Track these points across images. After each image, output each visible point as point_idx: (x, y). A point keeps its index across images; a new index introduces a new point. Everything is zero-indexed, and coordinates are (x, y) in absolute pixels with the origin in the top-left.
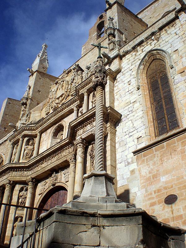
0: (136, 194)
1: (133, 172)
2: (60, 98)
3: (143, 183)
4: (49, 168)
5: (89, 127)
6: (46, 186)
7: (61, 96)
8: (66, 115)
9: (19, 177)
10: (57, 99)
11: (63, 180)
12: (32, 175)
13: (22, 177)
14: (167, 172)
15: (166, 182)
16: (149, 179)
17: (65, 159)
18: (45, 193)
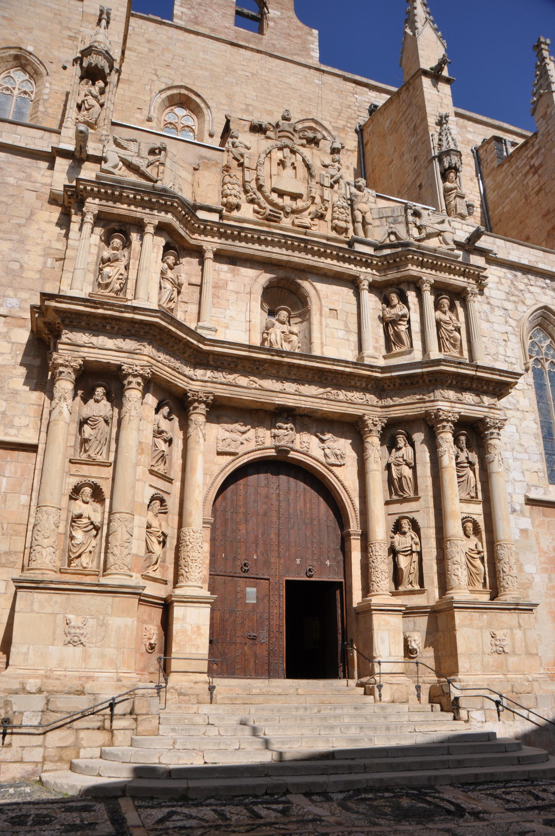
0: (533, 578)
1: (524, 532)
2: (287, 199)
3: (544, 563)
4: (290, 401)
5: (469, 397)
6: (245, 436)
7: (295, 197)
8: (321, 272)
9: (170, 370)
10: (274, 190)
13: (177, 375)
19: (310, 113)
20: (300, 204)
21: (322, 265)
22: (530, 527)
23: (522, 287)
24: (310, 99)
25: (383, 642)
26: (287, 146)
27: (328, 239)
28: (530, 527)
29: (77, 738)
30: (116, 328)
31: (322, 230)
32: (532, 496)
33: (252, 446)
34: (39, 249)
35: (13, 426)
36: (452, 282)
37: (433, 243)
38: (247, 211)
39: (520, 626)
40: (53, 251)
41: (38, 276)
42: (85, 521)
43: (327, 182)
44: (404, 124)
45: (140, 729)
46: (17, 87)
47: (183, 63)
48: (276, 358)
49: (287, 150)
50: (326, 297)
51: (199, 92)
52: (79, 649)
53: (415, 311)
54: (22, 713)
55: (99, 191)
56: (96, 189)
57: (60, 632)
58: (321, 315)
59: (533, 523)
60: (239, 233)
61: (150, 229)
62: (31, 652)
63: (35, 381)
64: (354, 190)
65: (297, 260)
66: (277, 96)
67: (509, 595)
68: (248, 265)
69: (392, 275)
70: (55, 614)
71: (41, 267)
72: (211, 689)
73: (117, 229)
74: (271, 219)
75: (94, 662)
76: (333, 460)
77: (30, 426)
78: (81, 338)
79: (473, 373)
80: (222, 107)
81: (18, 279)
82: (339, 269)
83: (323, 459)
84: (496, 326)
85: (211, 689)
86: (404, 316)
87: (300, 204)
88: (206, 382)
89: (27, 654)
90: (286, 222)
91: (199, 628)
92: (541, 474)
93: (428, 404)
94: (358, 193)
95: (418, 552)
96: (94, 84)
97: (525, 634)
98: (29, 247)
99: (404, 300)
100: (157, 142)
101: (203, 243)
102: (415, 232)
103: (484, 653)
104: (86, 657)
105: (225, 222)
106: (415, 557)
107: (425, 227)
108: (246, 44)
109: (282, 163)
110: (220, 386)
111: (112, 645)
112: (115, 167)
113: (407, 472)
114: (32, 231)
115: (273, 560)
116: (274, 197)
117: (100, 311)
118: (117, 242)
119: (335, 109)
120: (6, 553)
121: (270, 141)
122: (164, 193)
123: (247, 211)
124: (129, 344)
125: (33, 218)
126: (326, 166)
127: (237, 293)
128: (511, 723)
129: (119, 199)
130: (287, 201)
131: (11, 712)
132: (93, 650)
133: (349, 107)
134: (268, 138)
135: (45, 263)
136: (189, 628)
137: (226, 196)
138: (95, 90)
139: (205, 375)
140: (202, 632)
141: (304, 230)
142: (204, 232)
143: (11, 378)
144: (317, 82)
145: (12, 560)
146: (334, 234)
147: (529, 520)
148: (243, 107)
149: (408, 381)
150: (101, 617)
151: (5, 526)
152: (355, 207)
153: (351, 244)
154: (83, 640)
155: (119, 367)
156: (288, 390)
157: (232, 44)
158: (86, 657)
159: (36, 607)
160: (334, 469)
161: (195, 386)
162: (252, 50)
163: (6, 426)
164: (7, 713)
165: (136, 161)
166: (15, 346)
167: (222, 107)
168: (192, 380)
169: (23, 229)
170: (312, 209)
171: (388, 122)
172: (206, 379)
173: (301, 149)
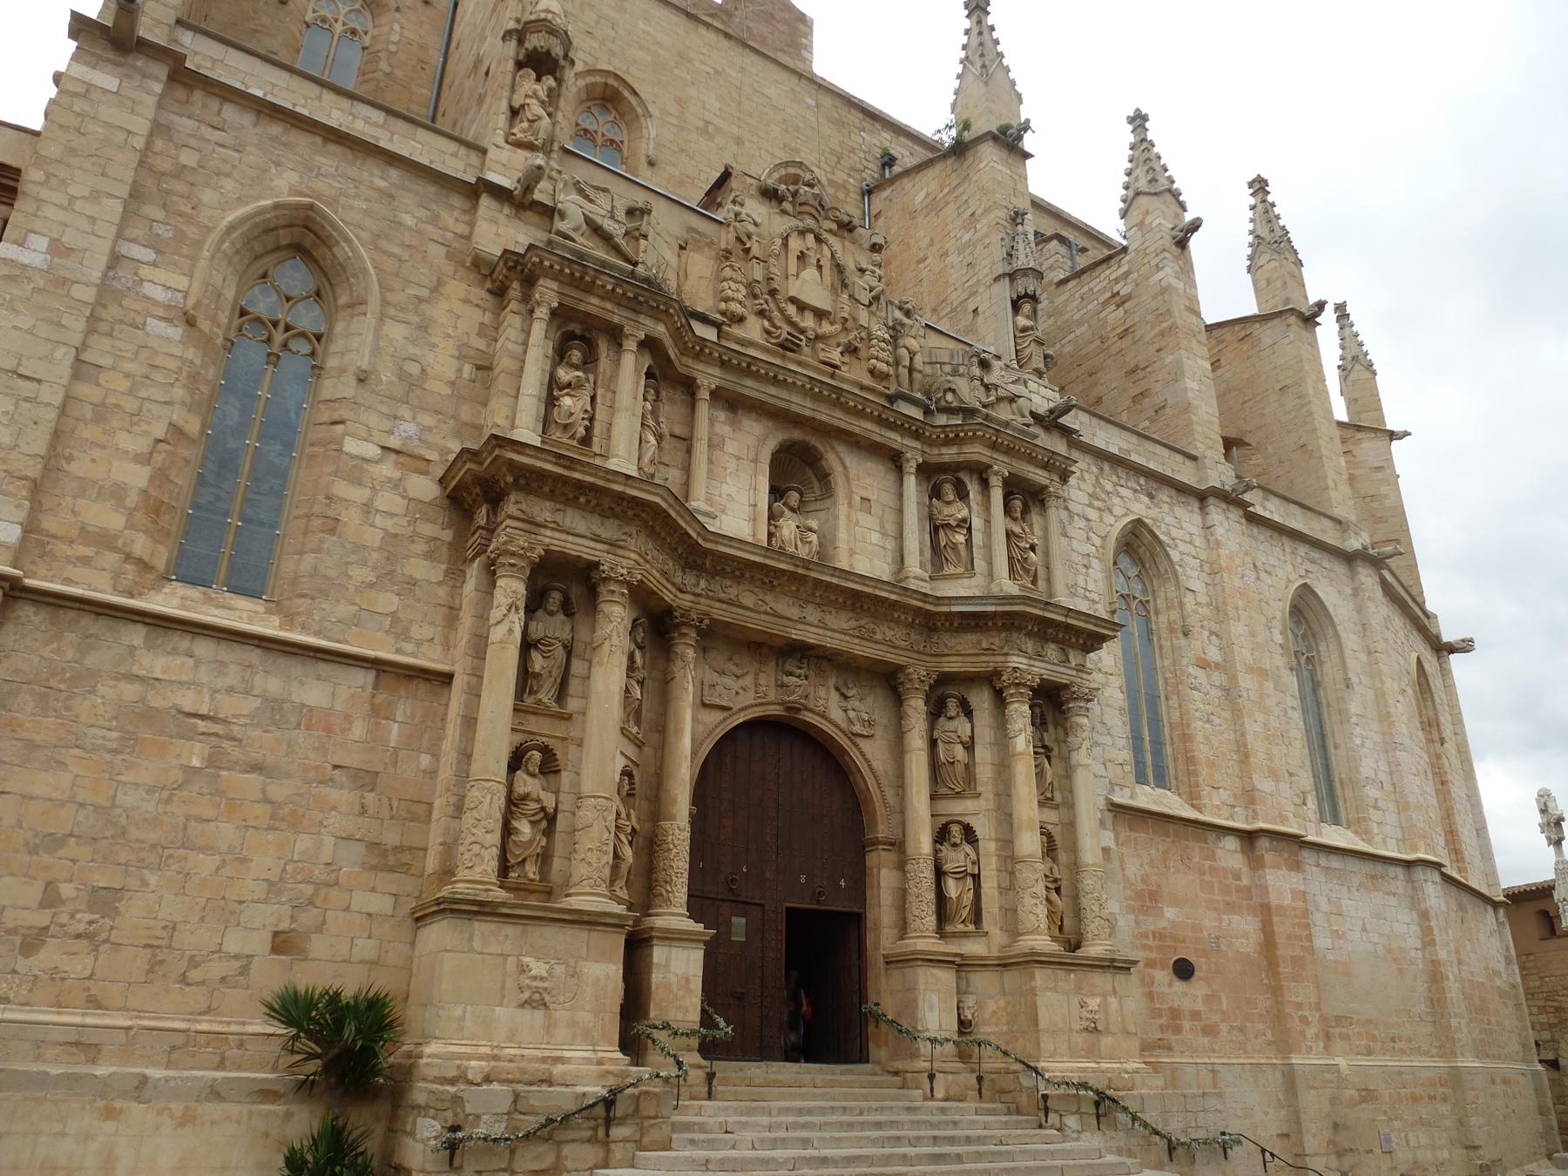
3: (1130, 898)
4: (810, 636)
6: (741, 682)
7: (820, 314)
10: (793, 300)
11: (836, 714)
12: (703, 600)
14: (1176, 902)
15: (1174, 924)
16: (1139, 896)
17: (891, 657)
18: (741, 718)
19: (797, 151)
20: (826, 328)
21: (857, 430)
22: (1113, 845)
23: (1109, 487)
24: (797, 129)
25: (931, 1008)
26: (811, 231)
27: (862, 388)
28: (1113, 845)
29: (558, 1156)
30: (594, 502)
31: (854, 373)
32: (1117, 799)
33: (749, 698)
34: (450, 346)
35: (408, 639)
36: (1031, 476)
37: (1003, 413)
38: (753, 329)
39: (1115, 992)
40: (472, 352)
41: (448, 391)
42: (534, 805)
43: (865, 297)
44: (952, 206)
45: (646, 1140)
46: (341, 18)
47: (612, 33)
48: (800, 571)
49: (810, 237)
50: (859, 481)
51: (636, 86)
52: (539, 1014)
53: (986, 518)
54: (478, 1117)
55: (561, 271)
56: (557, 267)
57: (510, 983)
58: (850, 505)
59: (1117, 840)
60: (749, 365)
61: (630, 344)
62: (468, 1016)
63: (444, 567)
64: (898, 314)
65: (823, 418)
66: (751, 115)
67: (1095, 949)
68: (754, 416)
69: (949, 454)
70: (504, 956)
71: (453, 377)
72: (711, 1076)
73: (579, 338)
74: (788, 346)
75: (561, 1033)
76: (857, 728)
77: (437, 640)
78: (542, 510)
79: (1062, 619)
80: (669, 119)
81: (418, 392)
82: (878, 439)
83: (843, 725)
84: (1075, 544)
85: (711, 1076)
86: (964, 520)
87: (826, 328)
88: (700, 595)
89: (462, 1019)
90: (806, 354)
91: (687, 980)
92: (1128, 768)
93: (999, 659)
94: (906, 321)
95: (973, 876)
96: (538, 79)
97: (1120, 1003)
98: (434, 340)
99: (963, 495)
100: (640, 198)
101: (695, 374)
102: (981, 393)
103: (1071, 1030)
104: (550, 1026)
105: (724, 343)
106: (969, 882)
107: (996, 387)
108: (709, 20)
109: (802, 257)
110: (718, 605)
111: (588, 1007)
112: (575, 230)
113: (960, 753)
114: (438, 312)
115: (768, 875)
116: (791, 310)
117: (577, 475)
118: (576, 355)
119: (832, 152)
120: (395, 848)
121: (786, 217)
122: (651, 286)
123: (753, 329)
124: (609, 530)
125: (441, 290)
126: (862, 271)
127: (738, 458)
128: (1113, 1133)
129: (589, 289)
130: (808, 322)
131: (462, 1116)
132: (560, 1015)
133: (853, 151)
134: (784, 212)
135: (460, 370)
136: (674, 979)
137: (726, 300)
138: (541, 90)
139: (697, 585)
140: (692, 986)
141: (830, 370)
142: (698, 356)
143: (407, 557)
144: (809, 101)
145: (404, 861)
146: (868, 381)
147: (1111, 834)
148: (701, 124)
149: (973, 623)
150: (572, 963)
151: (395, 804)
152: (901, 342)
153: (891, 399)
154: (547, 998)
155: (596, 565)
156: (810, 619)
157: (689, 16)
158: (550, 1026)
159: (477, 944)
160: (858, 740)
161: (684, 601)
162: (717, 30)
163: (398, 636)
164: (455, 1115)
165: (608, 225)
166: (413, 504)
167: (669, 119)
168: (681, 591)
169: (424, 306)
170: (843, 339)
171: (922, 195)
172: (698, 591)
173: (832, 239)
